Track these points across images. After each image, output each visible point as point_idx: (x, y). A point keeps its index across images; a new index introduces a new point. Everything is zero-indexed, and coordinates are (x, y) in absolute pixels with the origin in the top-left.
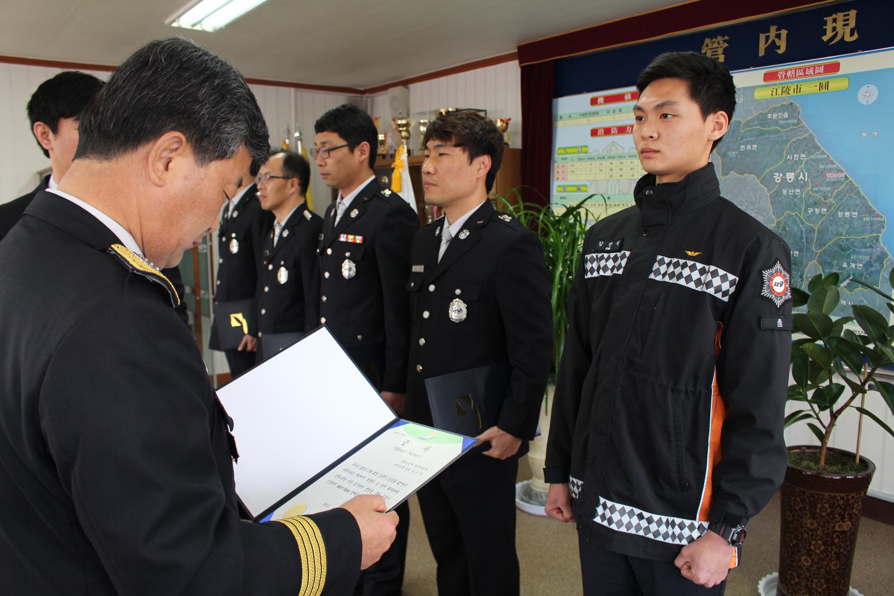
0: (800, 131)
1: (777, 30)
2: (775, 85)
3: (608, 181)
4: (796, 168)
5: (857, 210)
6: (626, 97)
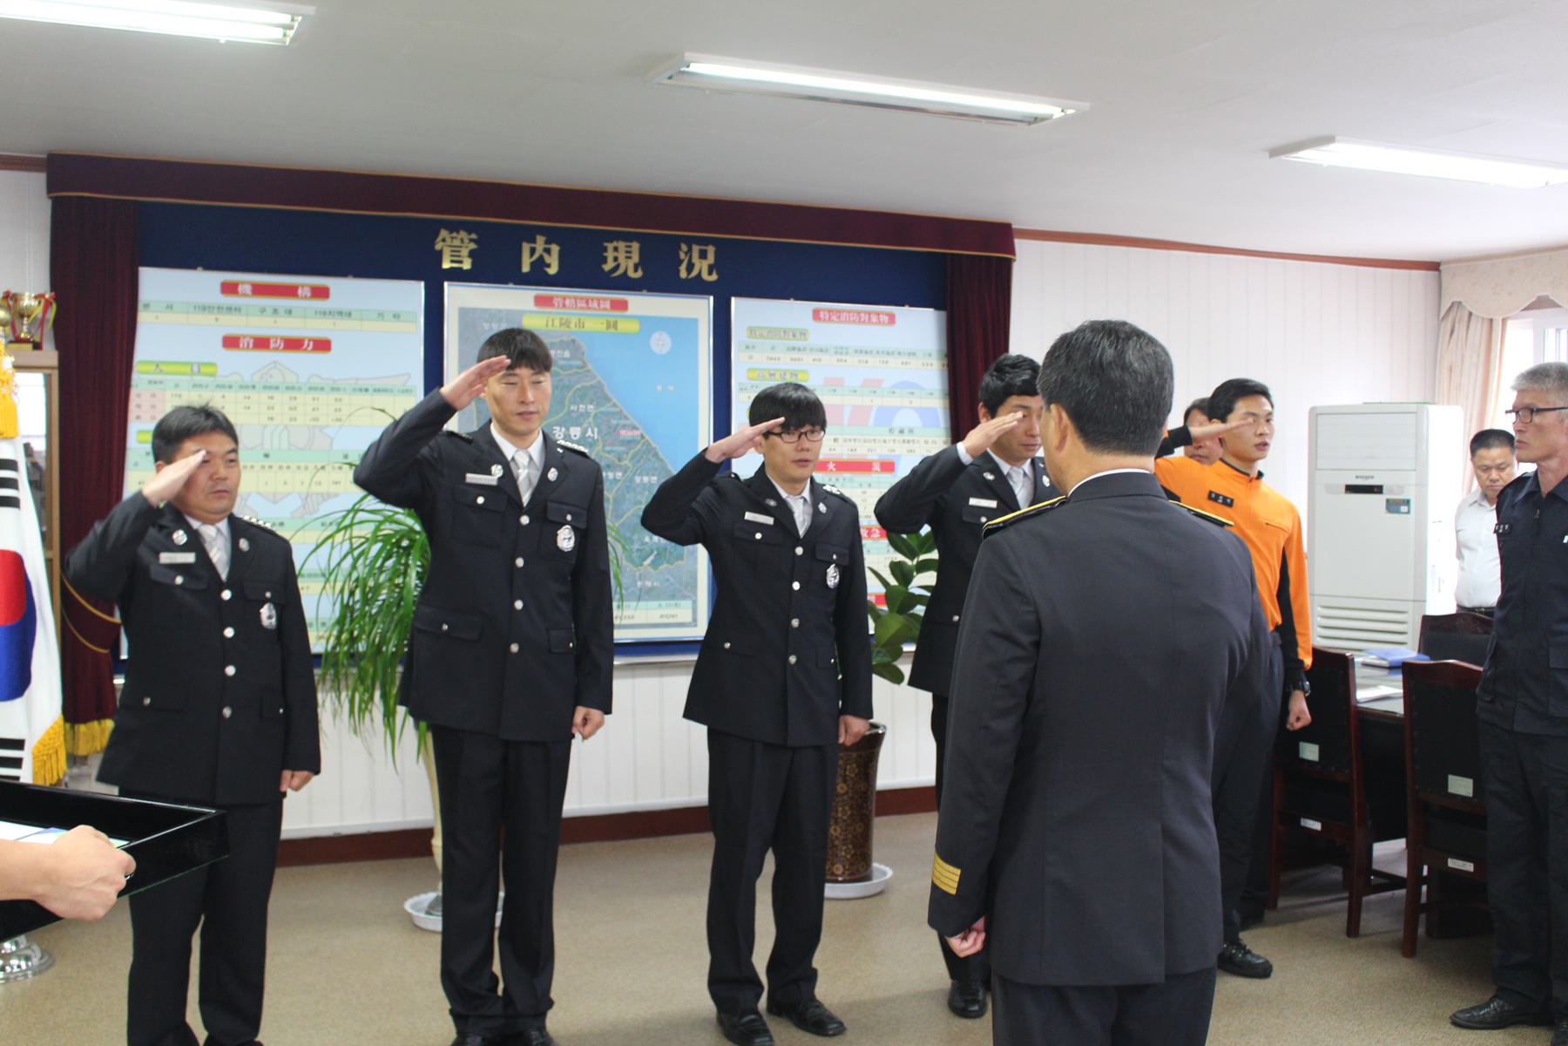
0: (586, 376)
1: (547, 242)
2: (550, 313)
3: (265, 427)
4: (582, 421)
5: (657, 473)
6: (300, 291)
